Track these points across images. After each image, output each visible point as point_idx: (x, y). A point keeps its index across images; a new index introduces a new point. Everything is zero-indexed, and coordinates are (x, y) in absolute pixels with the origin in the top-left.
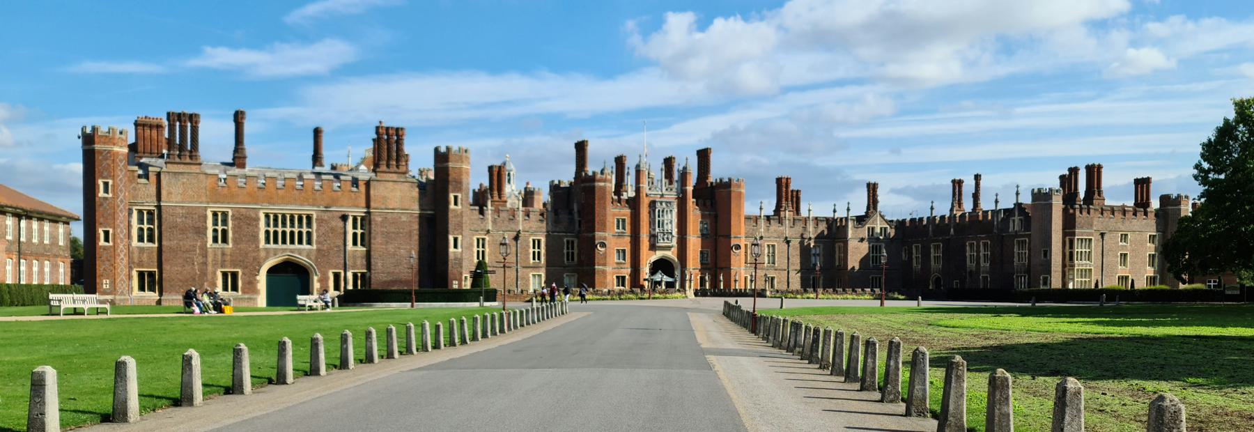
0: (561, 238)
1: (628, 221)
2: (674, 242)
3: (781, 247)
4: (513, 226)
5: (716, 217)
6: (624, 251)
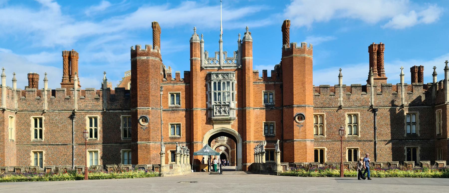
0: (117, 115)
1: (183, 95)
2: (233, 114)
3: (365, 117)
4: (68, 105)
5: (282, 86)
6: (179, 126)
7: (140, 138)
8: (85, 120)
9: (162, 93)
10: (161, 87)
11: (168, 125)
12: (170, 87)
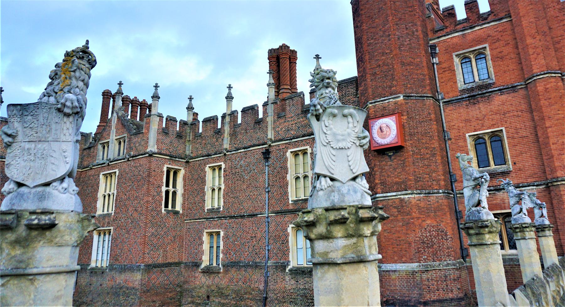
7: (383, 183)
8: (286, 160)
9: (436, 60)
10: (433, 47)
11: (465, 141)
12: (455, 40)
